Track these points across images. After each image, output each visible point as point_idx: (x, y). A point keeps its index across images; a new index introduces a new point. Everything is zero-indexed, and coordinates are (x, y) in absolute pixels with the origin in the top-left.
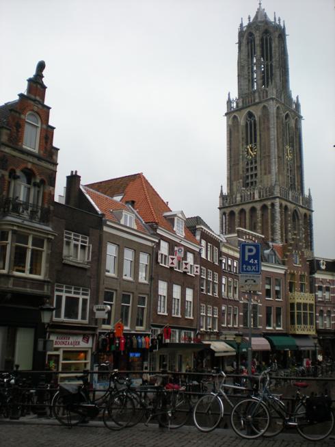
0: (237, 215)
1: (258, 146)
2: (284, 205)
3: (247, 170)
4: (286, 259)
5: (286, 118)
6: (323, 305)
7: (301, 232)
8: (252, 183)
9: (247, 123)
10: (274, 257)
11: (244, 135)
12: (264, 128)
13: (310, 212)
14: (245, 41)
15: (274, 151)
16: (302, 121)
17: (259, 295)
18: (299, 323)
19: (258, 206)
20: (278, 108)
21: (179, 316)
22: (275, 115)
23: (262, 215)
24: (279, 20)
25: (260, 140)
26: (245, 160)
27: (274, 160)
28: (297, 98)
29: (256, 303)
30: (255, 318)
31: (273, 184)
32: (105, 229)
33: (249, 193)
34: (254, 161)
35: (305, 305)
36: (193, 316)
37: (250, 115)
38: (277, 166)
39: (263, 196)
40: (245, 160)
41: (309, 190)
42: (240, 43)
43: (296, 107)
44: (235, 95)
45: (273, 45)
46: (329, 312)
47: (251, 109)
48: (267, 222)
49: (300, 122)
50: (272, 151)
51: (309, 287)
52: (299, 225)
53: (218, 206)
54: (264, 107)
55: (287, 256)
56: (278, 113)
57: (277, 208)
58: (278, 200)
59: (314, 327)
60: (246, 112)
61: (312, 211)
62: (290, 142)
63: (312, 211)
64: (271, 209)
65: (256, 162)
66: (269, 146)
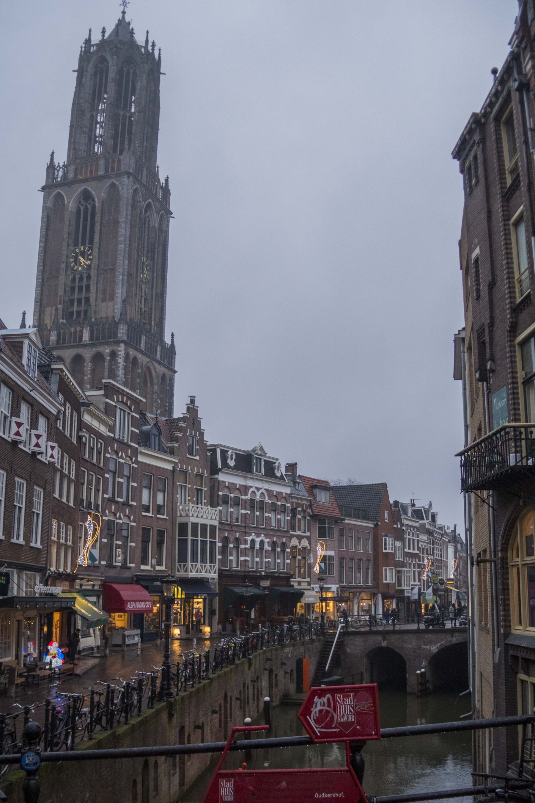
2: (131, 357)
4: (176, 445)
5: (146, 211)
6: (229, 528)
7: (155, 404)
8: (79, 313)
9: (79, 208)
10: (157, 438)
13: (170, 373)
17: (131, 506)
18: (194, 559)
19: (88, 354)
20: (135, 191)
21: (21, 541)
22: (130, 201)
23: (93, 370)
24: (153, 45)
25: (100, 242)
26: (69, 272)
28: (167, 180)
29: (126, 521)
30: (124, 547)
31: (117, 319)
33: (72, 330)
34: (85, 276)
35: (204, 526)
36: (42, 543)
37: (87, 196)
38: (125, 290)
39: (98, 339)
40: (69, 272)
41: (173, 335)
42: (81, 72)
43: (163, 194)
44: (61, 159)
45: (139, 85)
46: (237, 540)
49: (168, 221)
51: (208, 497)
52: (153, 392)
54: (113, 185)
55: (177, 439)
56: (134, 200)
57: (121, 361)
58: (122, 347)
59: (217, 566)
60: (82, 188)
61: (175, 372)
62: (148, 252)
63: (175, 372)
64: (110, 362)
65: (89, 277)
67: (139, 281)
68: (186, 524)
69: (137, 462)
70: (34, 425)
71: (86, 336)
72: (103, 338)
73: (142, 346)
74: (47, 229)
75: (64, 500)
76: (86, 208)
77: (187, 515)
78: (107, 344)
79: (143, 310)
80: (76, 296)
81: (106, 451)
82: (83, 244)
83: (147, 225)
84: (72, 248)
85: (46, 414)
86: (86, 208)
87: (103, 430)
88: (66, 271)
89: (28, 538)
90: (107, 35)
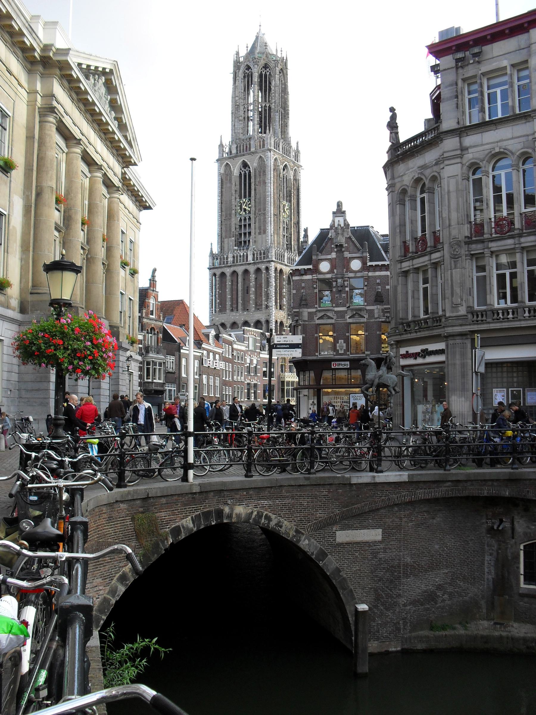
0: (228, 278)
2: (279, 270)
3: (241, 226)
5: (284, 170)
8: (245, 242)
9: (240, 173)
11: (238, 187)
12: (259, 182)
14: (241, 75)
16: (302, 171)
20: (276, 159)
21: (213, 395)
26: (238, 216)
28: (297, 143)
29: (255, 382)
30: (255, 393)
32: (182, 351)
33: (242, 254)
34: (247, 218)
37: (245, 165)
38: (272, 227)
39: (257, 258)
40: (238, 216)
44: (227, 140)
45: (273, 83)
47: (246, 159)
48: (261, 287)
50: (268, 209)
53: (208, 266)
54: (261, 157)
62: (287, 197)
65: (250, 218)
66: (265, 203)
67: (281, 218)
68: (284, 382)
69: (260, 357)
70: (214, 358)
71: (250, 258)
72: (261, 258)
73: (286, 260)
74: (222, 188)
75: (227, 379)
76: (245, 174)
77: (284, 378)
78: (262, 262)
79: (285, 237)
80: (243, 231)
81: (245, 356)
82: (245, 197)
83: (285, 179)
84: (238, 200)
85: (219, 354)
86: (245, 174)
87: (243, 348)
88: (236, 215)
89: (215, 394)
90: (249, 49)
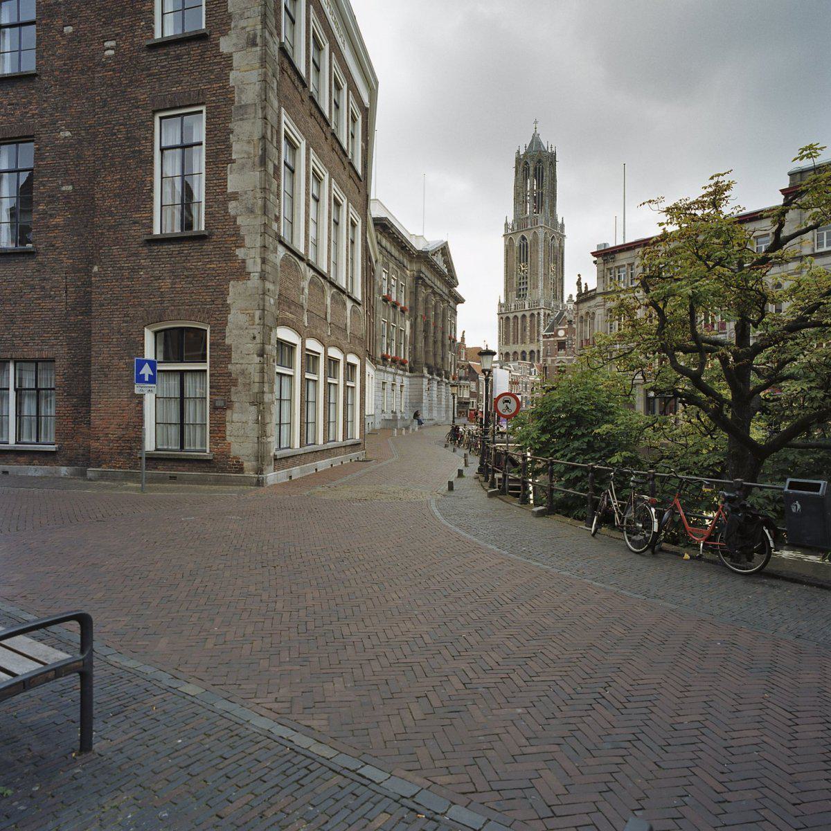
1: (529, 265)
3: (520, 283)
9: (520, 245)
11: (518, 254)
12: (534, 250)
14: (521, 169)
15: (541, 270)
16: (566, 240)
19: (528, 314)
27: (541, 278)
37: (523, 238)
44: (511, 220)
65: (527, 278)
66: (538, 266)
